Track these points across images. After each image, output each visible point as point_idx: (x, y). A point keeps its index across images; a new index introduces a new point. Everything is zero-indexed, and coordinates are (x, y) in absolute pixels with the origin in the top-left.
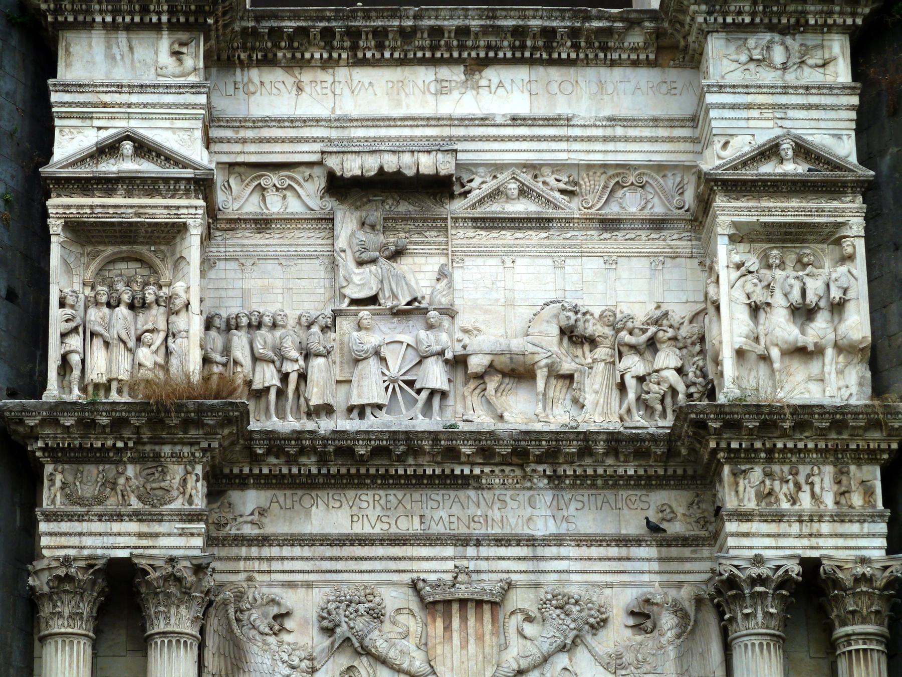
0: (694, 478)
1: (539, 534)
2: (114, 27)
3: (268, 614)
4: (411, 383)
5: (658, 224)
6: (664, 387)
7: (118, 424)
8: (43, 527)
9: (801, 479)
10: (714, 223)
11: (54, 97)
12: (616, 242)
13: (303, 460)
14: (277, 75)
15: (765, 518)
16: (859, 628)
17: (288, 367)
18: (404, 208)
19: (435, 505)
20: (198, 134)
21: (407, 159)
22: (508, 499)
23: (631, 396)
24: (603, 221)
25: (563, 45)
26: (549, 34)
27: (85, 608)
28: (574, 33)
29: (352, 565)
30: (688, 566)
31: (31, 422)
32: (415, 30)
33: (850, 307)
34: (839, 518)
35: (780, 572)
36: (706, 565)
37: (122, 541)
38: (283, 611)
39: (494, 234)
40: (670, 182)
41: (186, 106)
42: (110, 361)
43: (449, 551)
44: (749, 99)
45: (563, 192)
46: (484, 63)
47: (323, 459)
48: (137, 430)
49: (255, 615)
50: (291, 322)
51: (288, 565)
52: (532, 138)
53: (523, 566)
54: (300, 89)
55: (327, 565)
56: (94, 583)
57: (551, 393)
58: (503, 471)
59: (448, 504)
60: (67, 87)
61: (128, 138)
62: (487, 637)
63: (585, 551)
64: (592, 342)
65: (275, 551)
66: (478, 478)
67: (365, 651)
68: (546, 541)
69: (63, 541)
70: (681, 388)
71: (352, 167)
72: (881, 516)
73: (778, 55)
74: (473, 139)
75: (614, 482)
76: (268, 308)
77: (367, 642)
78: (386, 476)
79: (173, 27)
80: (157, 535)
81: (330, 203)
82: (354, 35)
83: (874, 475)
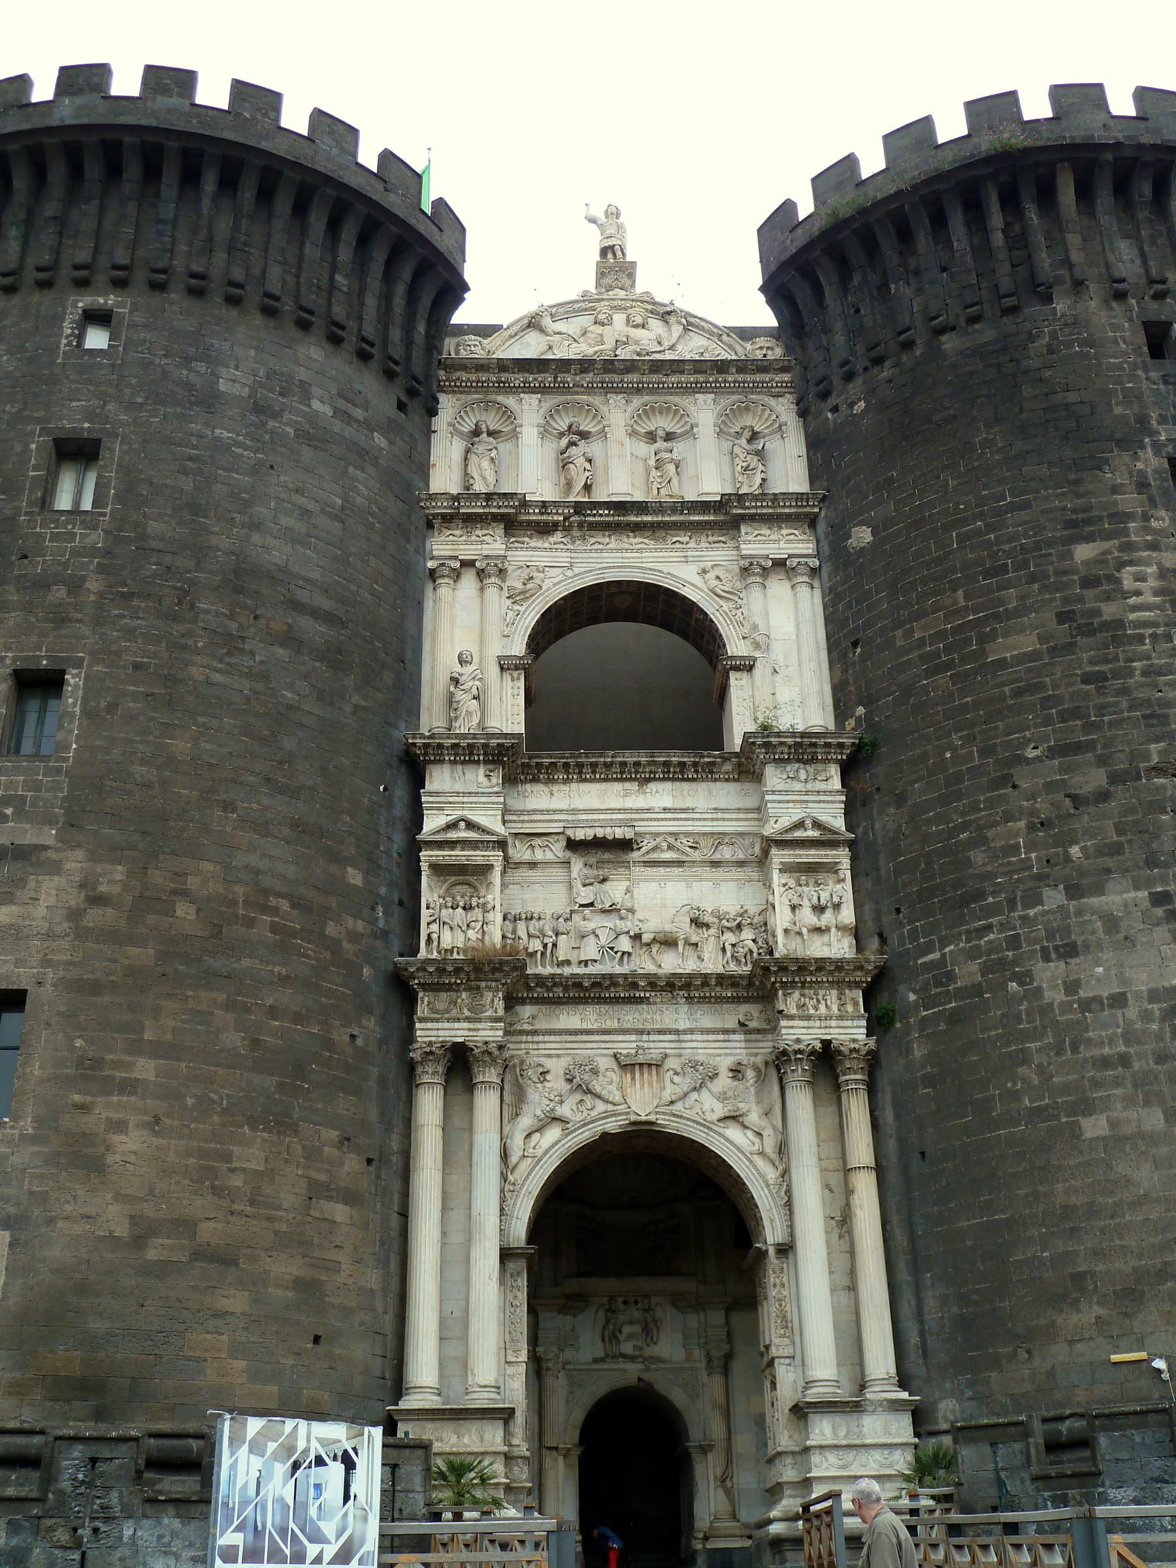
0: (763, 997)
1: (681, 1028)
2: (455, 762)
4: (611, 948)
5: (741, 864)
6: (746, 949)
7: (458, 970)
8: (418, 1025)
9: (820, 997)
10: (771, 863)
11: (423, 799)
12: (719, 873)
13: (555, 989)
14: (540, 787)
15: (801, 1018)
16: (852, 1077)
17: (547, 940)
18: (607, 856)
20: (500, 818)
21: (609, 830)
23: (729, 954)
26: (682, 765)
27: (440, 1069)
28: (695, 764)
29: (582, 1046)
30: (760, 1045)
31: (411, 970)
32: (612, 762)
33: (844, 906)
34: (841, 1018)
36: (770, 1044)
37: (460, 1033)
39: (655, 869)
40: (747, 841)
42: (453, 938)
43: (633, 1037)
44: (788, 798)
46: (648, 780)
47: (566, 988)
48: (468, 974)
50: (548, 916)
51: (548, 1046)
52: (674, 819)
56: (445, 1055)
60: (430, 794)
63: (705, 1037)
64: (708, 926)
65: (541, 1038)
67: (589, 1091)
68: (685, 1032)
69: (428, 1033)
70: (755, 950)
71: (579, 835)
73: (803, 775)
74: (643, 820)
75: (720, 1000)
76: (536, 910)
77: (590, 1086)
78: (600, 998)
79: (486, 762)
80: (478, 1030)
81: (568, 854)
82: (580, 766)
83: (859, 995)
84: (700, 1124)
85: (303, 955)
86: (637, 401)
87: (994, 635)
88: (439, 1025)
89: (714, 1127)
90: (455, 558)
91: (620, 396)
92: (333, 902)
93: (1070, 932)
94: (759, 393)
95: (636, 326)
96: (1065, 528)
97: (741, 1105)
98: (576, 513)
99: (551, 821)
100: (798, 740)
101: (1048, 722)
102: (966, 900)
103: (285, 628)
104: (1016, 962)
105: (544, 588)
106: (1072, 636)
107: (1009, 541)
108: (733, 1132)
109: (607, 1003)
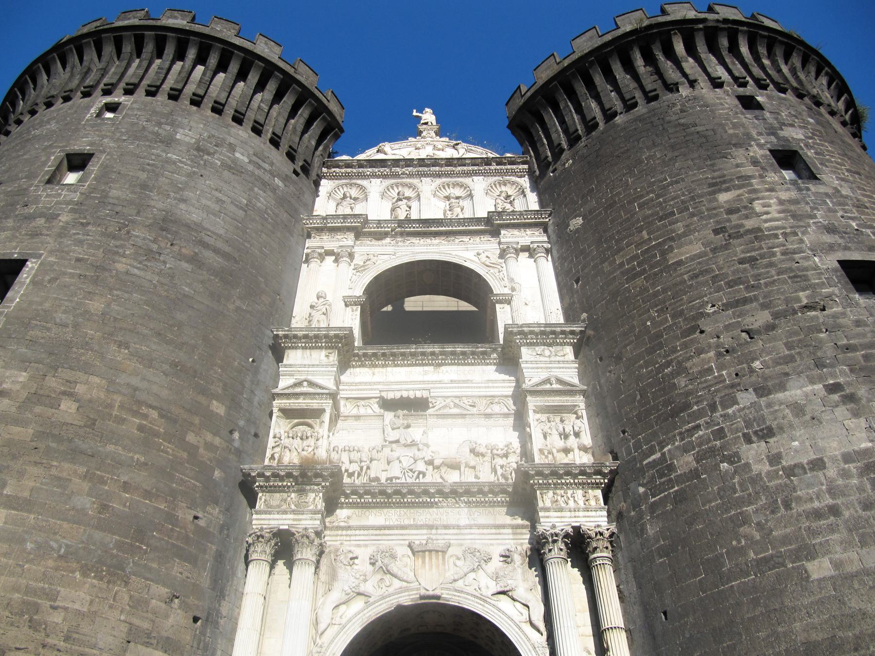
4: (411, 470)
7: (289, 475)
12: (491, 421)
17: (363, 464)
27: (268, 550)
31: (253, 474)
35: (564, 531)
38: (354, 556)
41: (329, 371)
43: (425, 531)
44: (537, 365)
45: (471, 406)
49: (342, 557)
50: (366, 450)
51: (358, 538)
52: (458, 387)
53: (455, 537)
54: (374, 374)
57: (466, 473)
60: (286, 366)
63: (481, 531)
64: (483, 455)
65: (353, 532)
66: (436, 503)
71: (390, 396)
72: (604, 508)
73: (547, 353)
74: (437, 388)
77: (389, 568)
80: (300, 520)
81: (382, 411)
82: (393, 355)
83: (599, 493)
85: (162, 451)
86: (439, 181)
87: (671, 249)
88: (272, 516)
89: (488, 600)
90: (323, 247)
91: (428, 179)
92: (197, 420)
93: (764, 419)
94: (510, 176)
95: (439, 150)
96: (709, 187)
97: (510, 582)
98: (399, 227)
99: (372, 389)
100: (543, 329)
101: (719, 289)
102: (675, 413)
103: (192, 253)
104: (722, 448)
105: (377, 263)
106: (726, 240)
107: (673, 199)
108: (504, 603)
109: (405, 507)
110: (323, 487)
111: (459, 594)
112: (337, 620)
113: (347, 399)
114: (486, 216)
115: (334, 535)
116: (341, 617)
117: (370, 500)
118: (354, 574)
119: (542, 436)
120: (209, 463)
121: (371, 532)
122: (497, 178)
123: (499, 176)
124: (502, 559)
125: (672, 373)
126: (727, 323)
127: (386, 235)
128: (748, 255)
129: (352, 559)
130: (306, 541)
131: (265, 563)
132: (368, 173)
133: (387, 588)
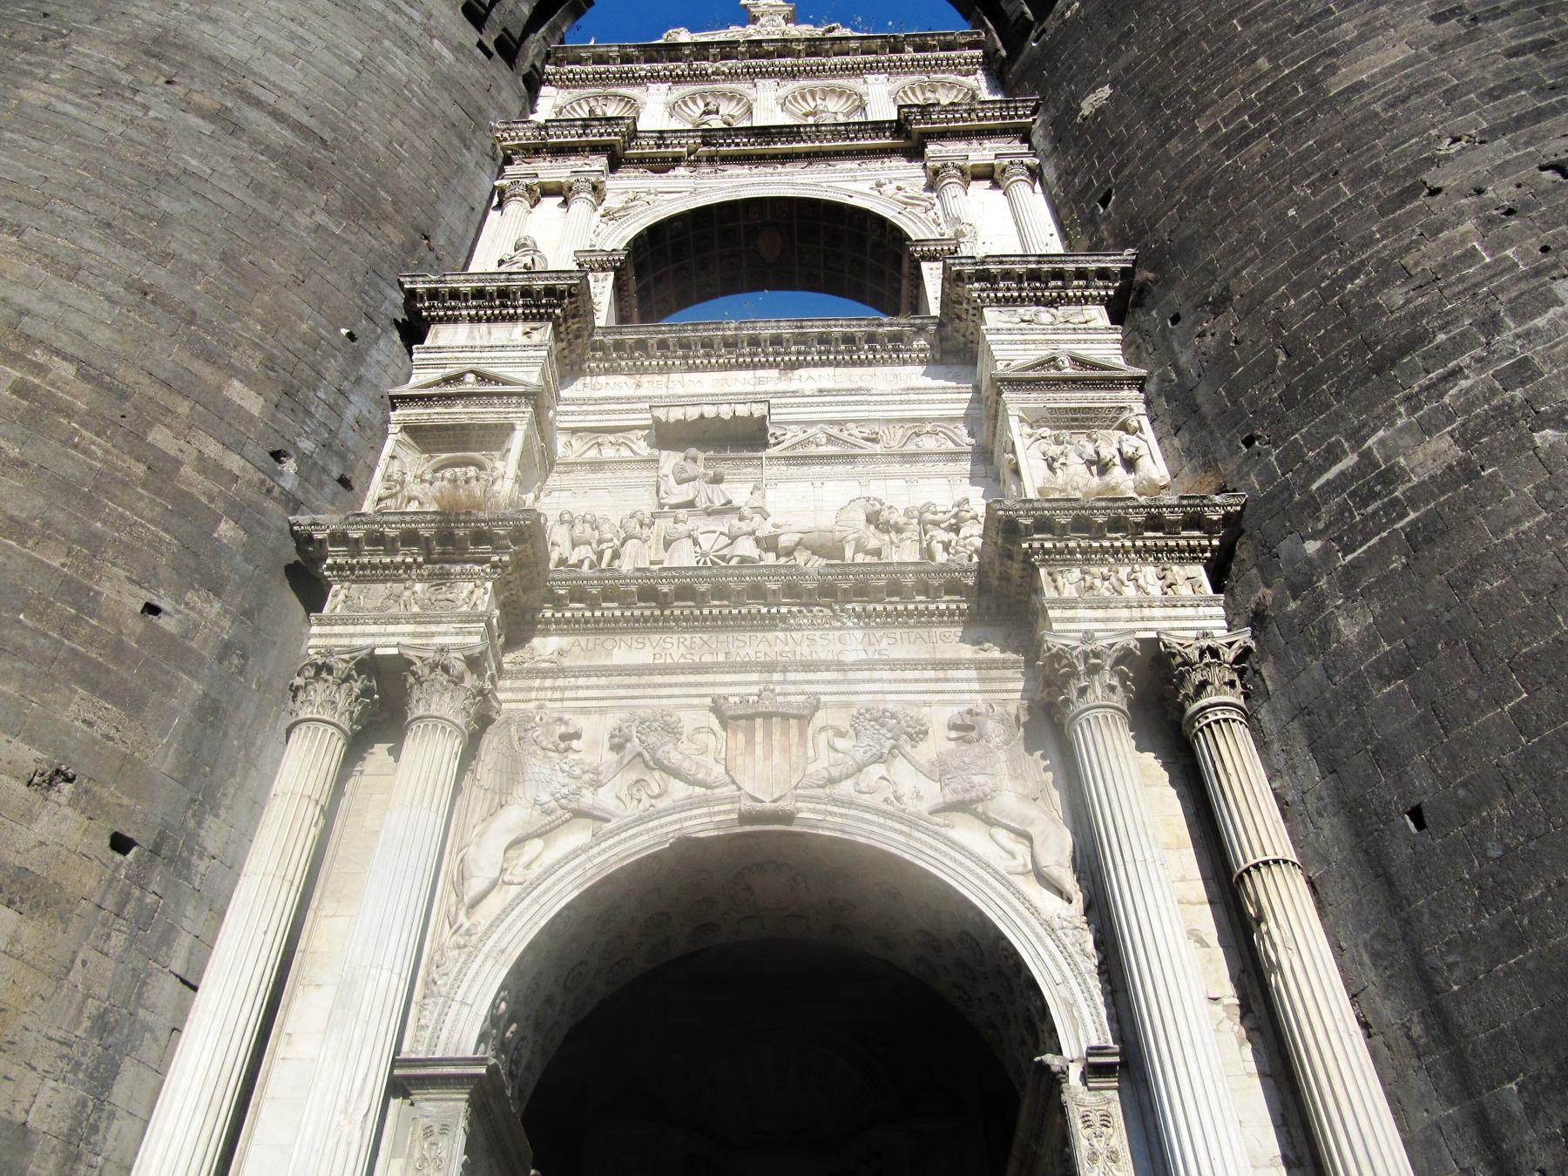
3: (553, 732)
19: (741, 644)
22: (817, 638)
24: (903, 455)
25: (863, 349)
27: (341, 699)
29: (651, 692)
38: (571, 730)
41: (529, 358)
43: (755, 677)
51: (581, 693)
55: (623, 692)
58: (811, 611)
59: (754, 644)
61: (472, 372)
62: (794, 749)
63: (898, 674)
66: (784, 619)
74: (786, 406)
77: (659, 754)
80: (433, 635)
81: (656, 452)
82: (685, 345)
83: (1198, 571)
84: (891, 816)
85: (75, 447)
86: (791, 86)
87: (1332, 70)
88: (359, 629)
92: (184, 407)
94: (943, 72)
97: (976, 779)
100: (1034, 266)
101: (1466, 108)
103: (218, 107)
109: (704, 629)
110: (494, 566)
111: (843, 811)
112: (517, 873)
113: (574, 431)
114: (895, 117)
115: (521, 690)
116: (528, 866)
117: (618, 613)
118: (566, 767)
119: (1044, 464)
120: (204, 500)
121: (616, 680)
122: (916, 77)
123: (921, 73)
124: (954, 734)
125: (1366, 287)
126: (1498, 162)
127: (677, 160)
128: (1530, 39)
129: (564, 737)
130: (444, 678)
131: (331, 729)
132: (643, 73)
133: (653, 801)
